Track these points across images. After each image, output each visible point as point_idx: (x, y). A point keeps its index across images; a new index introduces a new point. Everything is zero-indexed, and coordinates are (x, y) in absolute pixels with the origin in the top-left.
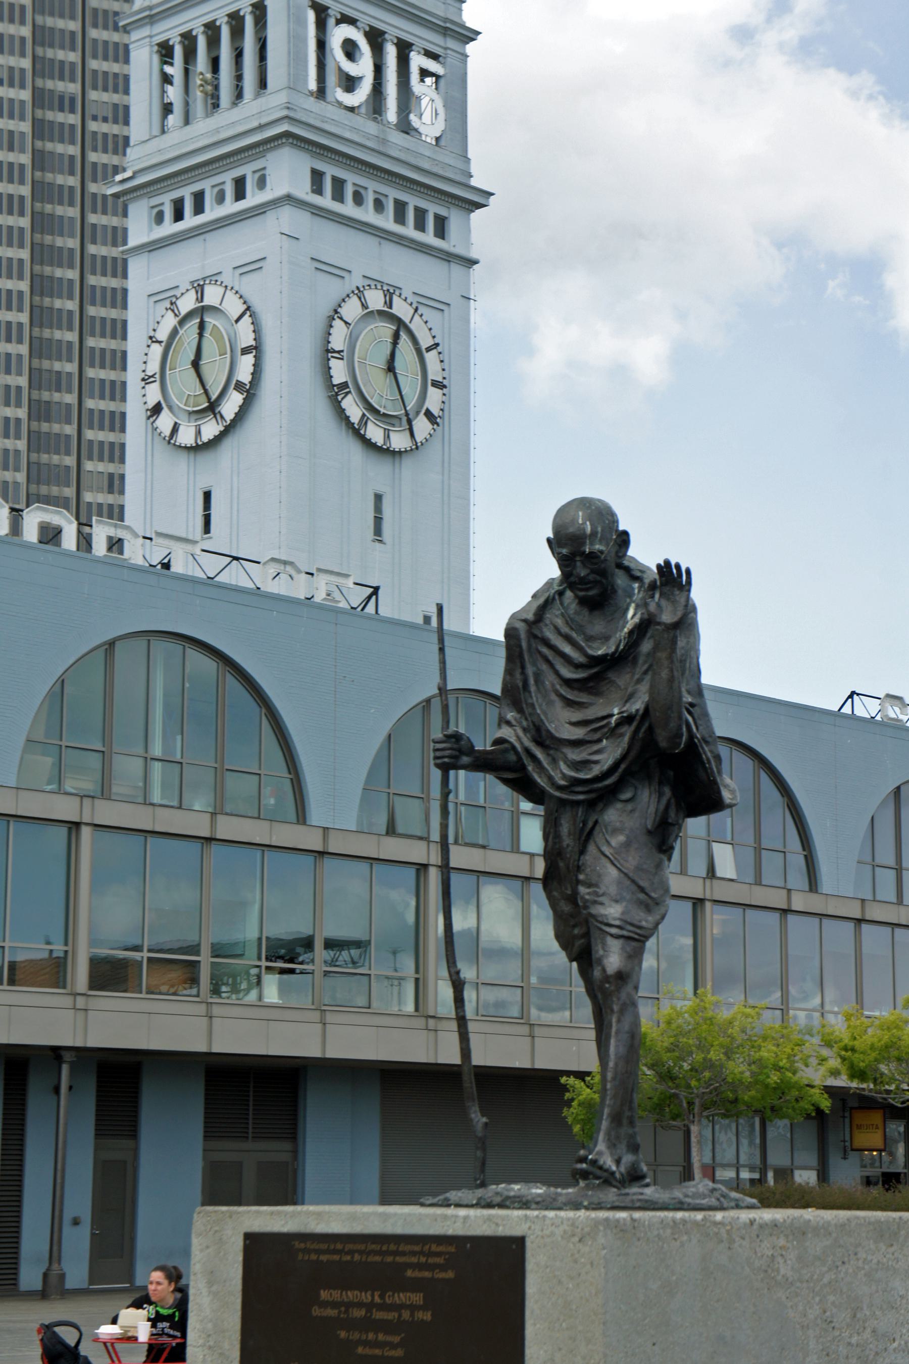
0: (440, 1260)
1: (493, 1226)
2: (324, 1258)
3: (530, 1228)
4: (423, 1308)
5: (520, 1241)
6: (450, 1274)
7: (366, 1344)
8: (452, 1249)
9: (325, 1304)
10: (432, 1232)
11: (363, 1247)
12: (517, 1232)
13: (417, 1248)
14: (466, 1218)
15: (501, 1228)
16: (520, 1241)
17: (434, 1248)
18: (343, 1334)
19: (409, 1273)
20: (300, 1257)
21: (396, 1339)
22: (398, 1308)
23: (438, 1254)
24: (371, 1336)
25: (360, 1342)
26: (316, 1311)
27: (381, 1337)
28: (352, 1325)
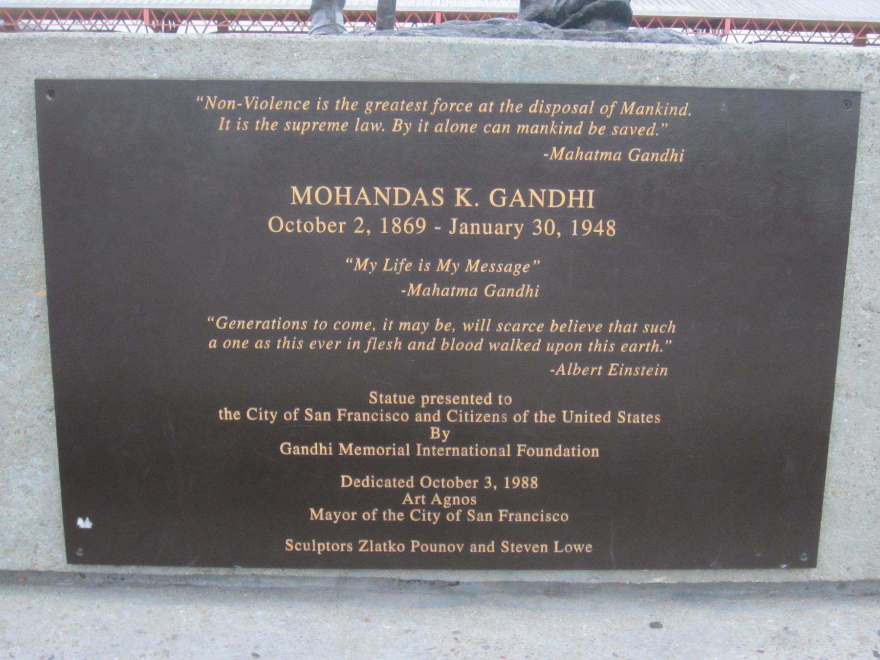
0: (651, 132)
1: (773, 74)
2: (299, 127)
3: (868, 78)
4: (595, 215)
5: (849, 101)
6: (674, 156)
7: (427, 279)
8: (683, 112)
9: (307, 212)
10: (602, 80)
11: (421, 106)
12: (841, 83)
13: (584, 109)
14: (697, 59)
15: (792, 77)
16: (849, 101)
17: (628, 108)
18: (362, 265)
19: (557, 154)
20: (224, 124)
21: (519, 269)
22: (525, 216)
23: (645, 121)
24: (444, 265)
25: (414, 277)
26: (278, 225)
27: (473, 266)
28: (381, 246)
